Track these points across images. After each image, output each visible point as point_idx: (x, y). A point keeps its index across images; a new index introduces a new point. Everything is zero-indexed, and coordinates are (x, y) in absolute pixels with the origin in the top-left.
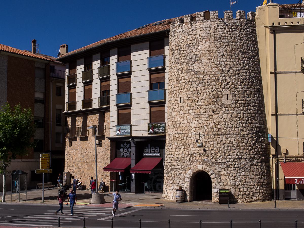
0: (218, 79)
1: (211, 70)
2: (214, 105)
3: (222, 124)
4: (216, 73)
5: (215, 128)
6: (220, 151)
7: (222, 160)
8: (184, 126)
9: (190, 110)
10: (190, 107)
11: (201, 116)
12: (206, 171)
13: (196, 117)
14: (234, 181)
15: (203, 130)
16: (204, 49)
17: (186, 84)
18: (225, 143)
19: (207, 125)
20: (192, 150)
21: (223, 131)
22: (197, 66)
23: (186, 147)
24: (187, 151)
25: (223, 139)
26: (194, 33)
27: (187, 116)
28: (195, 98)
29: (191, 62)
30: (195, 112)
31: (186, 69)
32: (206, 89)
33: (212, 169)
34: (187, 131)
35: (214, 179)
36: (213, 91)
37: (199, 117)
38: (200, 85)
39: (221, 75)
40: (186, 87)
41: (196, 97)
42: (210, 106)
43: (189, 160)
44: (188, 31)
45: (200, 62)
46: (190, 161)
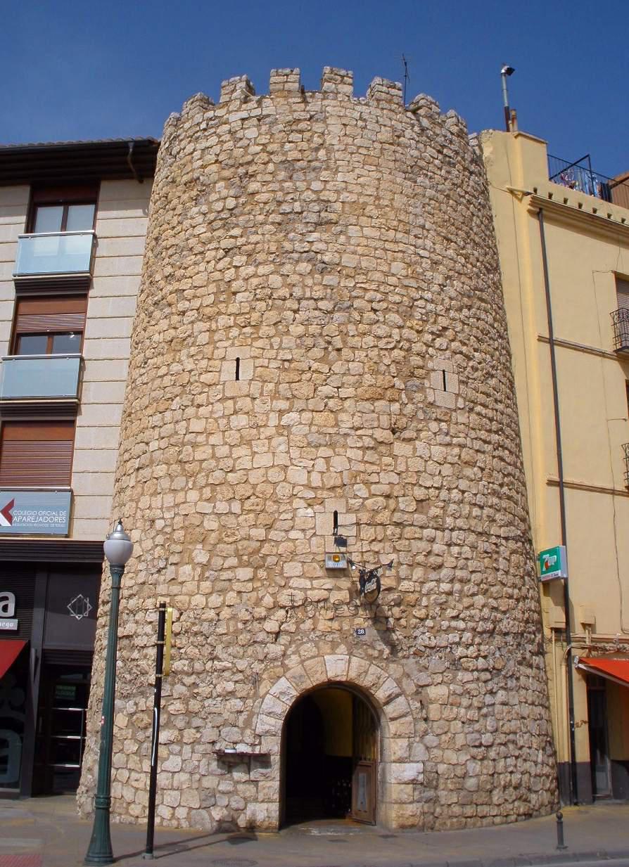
0: (411, 307)
1: (385, 268)
2: (397, 404)
3: (428, 484)
4: (406, 282)
5: (404, 496)
6: (424, 599)
7: (432, 637)
8: (252, 480)
9: (289, 411)
10: (288, 399)
11: (342, 440)
12: (366, 682)
13: (320, 445)
14: (477, 726)
15: (352, 501)
16: (359, 187)
17: (270, 308)
18: (440, 567)
19: (367, 484)
20: (295, 589)
21: (434, 511)
22: (326, 243)
23: (262, 573)
24: (271, 590)
25: (437, 548)
26: (318, 127)
27: (269, 438)
28: (315, 366)
29: (300, 227)
30: (312, 423)
31: (273, 249)
32: (365, 334)
33: (394, 676)
34: (269, 503)
35: (403, 720)
36: (392, 349)
37: (331, 445)
38: (336, 315)
39: (420, 292)
40: (272, 316)
41: (320, 360)
42: (380, 404)
43: (278, 634)
44: (290, 118)
45: (339, 228)
46: (284, 639)
